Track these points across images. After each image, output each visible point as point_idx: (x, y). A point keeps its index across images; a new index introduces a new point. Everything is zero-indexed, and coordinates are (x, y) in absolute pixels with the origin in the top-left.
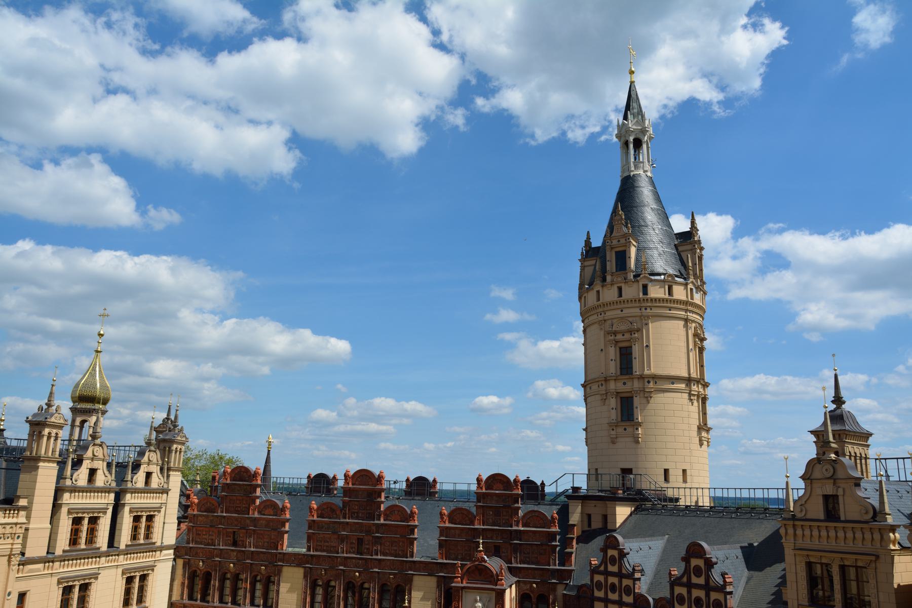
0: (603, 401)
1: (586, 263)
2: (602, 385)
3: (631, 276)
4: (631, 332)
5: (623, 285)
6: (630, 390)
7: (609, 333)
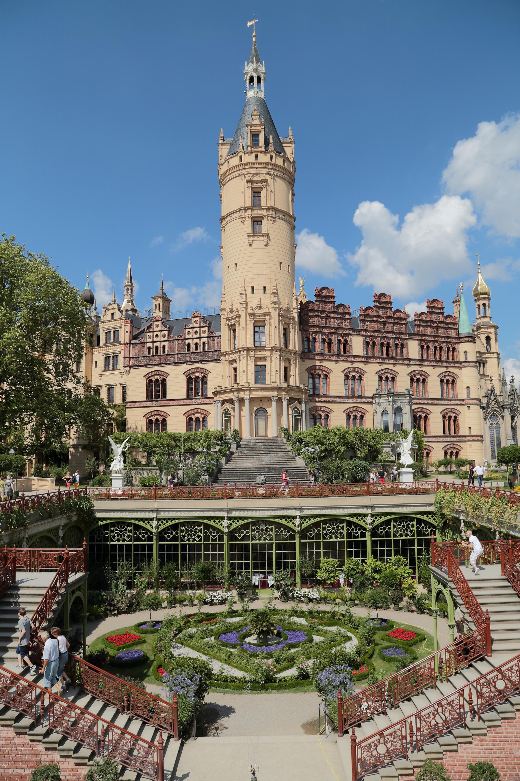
2: (242, 212)
3: (263, 149)
4: (262, 181)
5: (259, 154)
7: (248, 182)
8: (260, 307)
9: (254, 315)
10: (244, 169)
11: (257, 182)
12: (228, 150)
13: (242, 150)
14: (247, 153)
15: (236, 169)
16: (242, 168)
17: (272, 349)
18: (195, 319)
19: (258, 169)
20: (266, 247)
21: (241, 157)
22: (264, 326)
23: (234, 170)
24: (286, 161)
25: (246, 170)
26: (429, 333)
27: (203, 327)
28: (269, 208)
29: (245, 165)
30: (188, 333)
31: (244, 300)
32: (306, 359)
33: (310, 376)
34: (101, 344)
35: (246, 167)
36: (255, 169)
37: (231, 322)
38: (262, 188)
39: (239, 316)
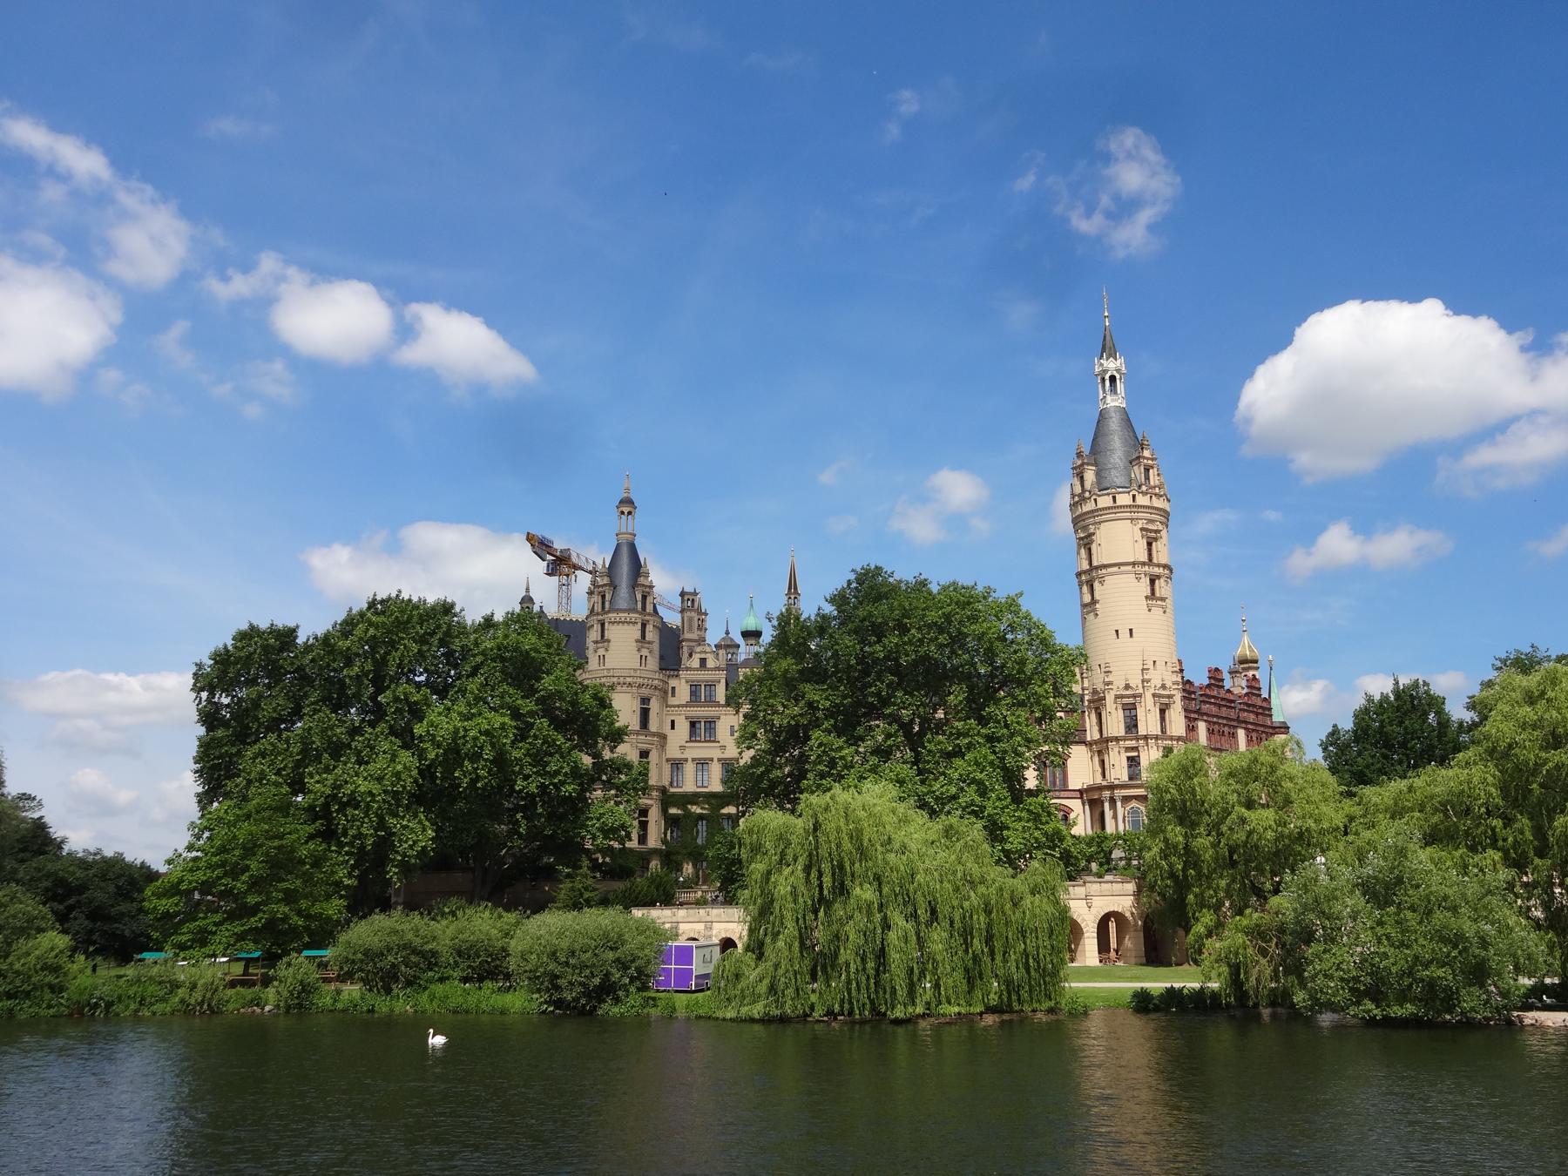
10: (1138, 512)
21: (1134, 496)
25: (1140, 514)
26: (1251, 720)
35: (1140, 510)
37: (1125, 701)
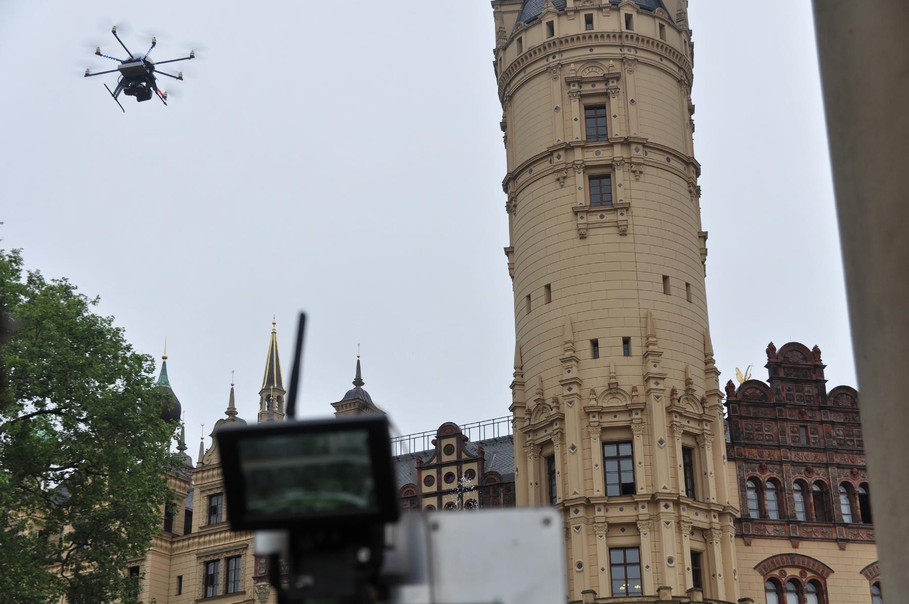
0: (562, 180)
1: (504, 9)
2: (559, 157)
4: (606, 80)
5: (595, 14)
6: (610, 162)
8: (613, 389)
9: (601, 413)
11: (593, 81)
12: (516, 15)
13: (552, 8)
14: (566, 14)
15: (539, 56)
16: (550, 51)
17: (654, 500)
18: (445, 442)
19: (596, 51)
20: (624, 239)
21: (551, 25)
22: (630, 442)
23: (534, 58)
24: (668, 30)
27: (467, 462)
28: (626, 143)
29: (561, 42)
30: (429, 481)
31: (574, 374)
32: (755, 536)
33: (771, 586)
34: (195, 529)
36: (587, 51)
37: (542, 436)
38: (606, 95)
39: (562, 419)
